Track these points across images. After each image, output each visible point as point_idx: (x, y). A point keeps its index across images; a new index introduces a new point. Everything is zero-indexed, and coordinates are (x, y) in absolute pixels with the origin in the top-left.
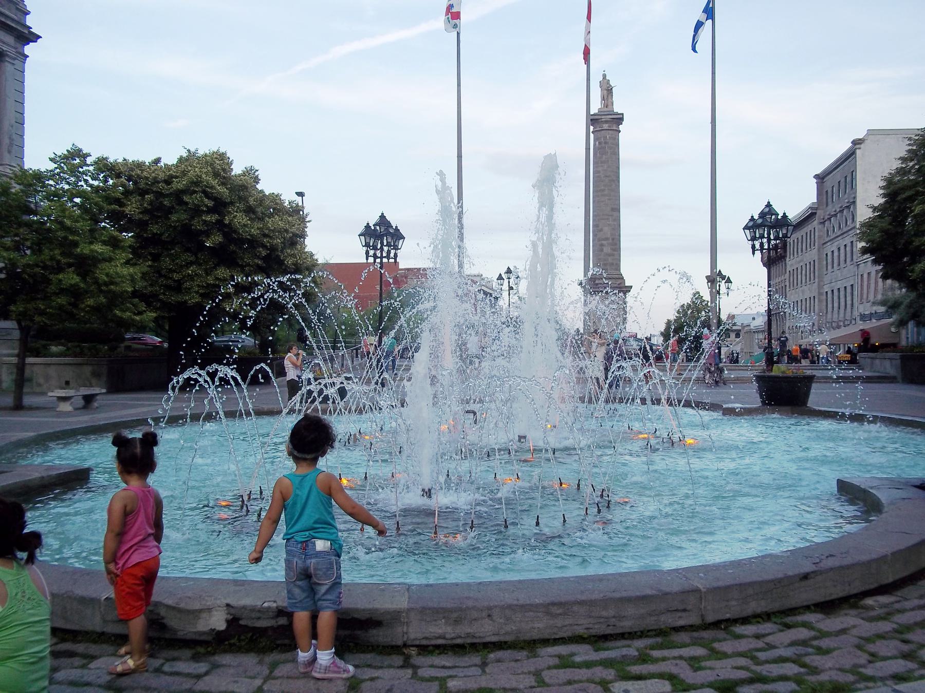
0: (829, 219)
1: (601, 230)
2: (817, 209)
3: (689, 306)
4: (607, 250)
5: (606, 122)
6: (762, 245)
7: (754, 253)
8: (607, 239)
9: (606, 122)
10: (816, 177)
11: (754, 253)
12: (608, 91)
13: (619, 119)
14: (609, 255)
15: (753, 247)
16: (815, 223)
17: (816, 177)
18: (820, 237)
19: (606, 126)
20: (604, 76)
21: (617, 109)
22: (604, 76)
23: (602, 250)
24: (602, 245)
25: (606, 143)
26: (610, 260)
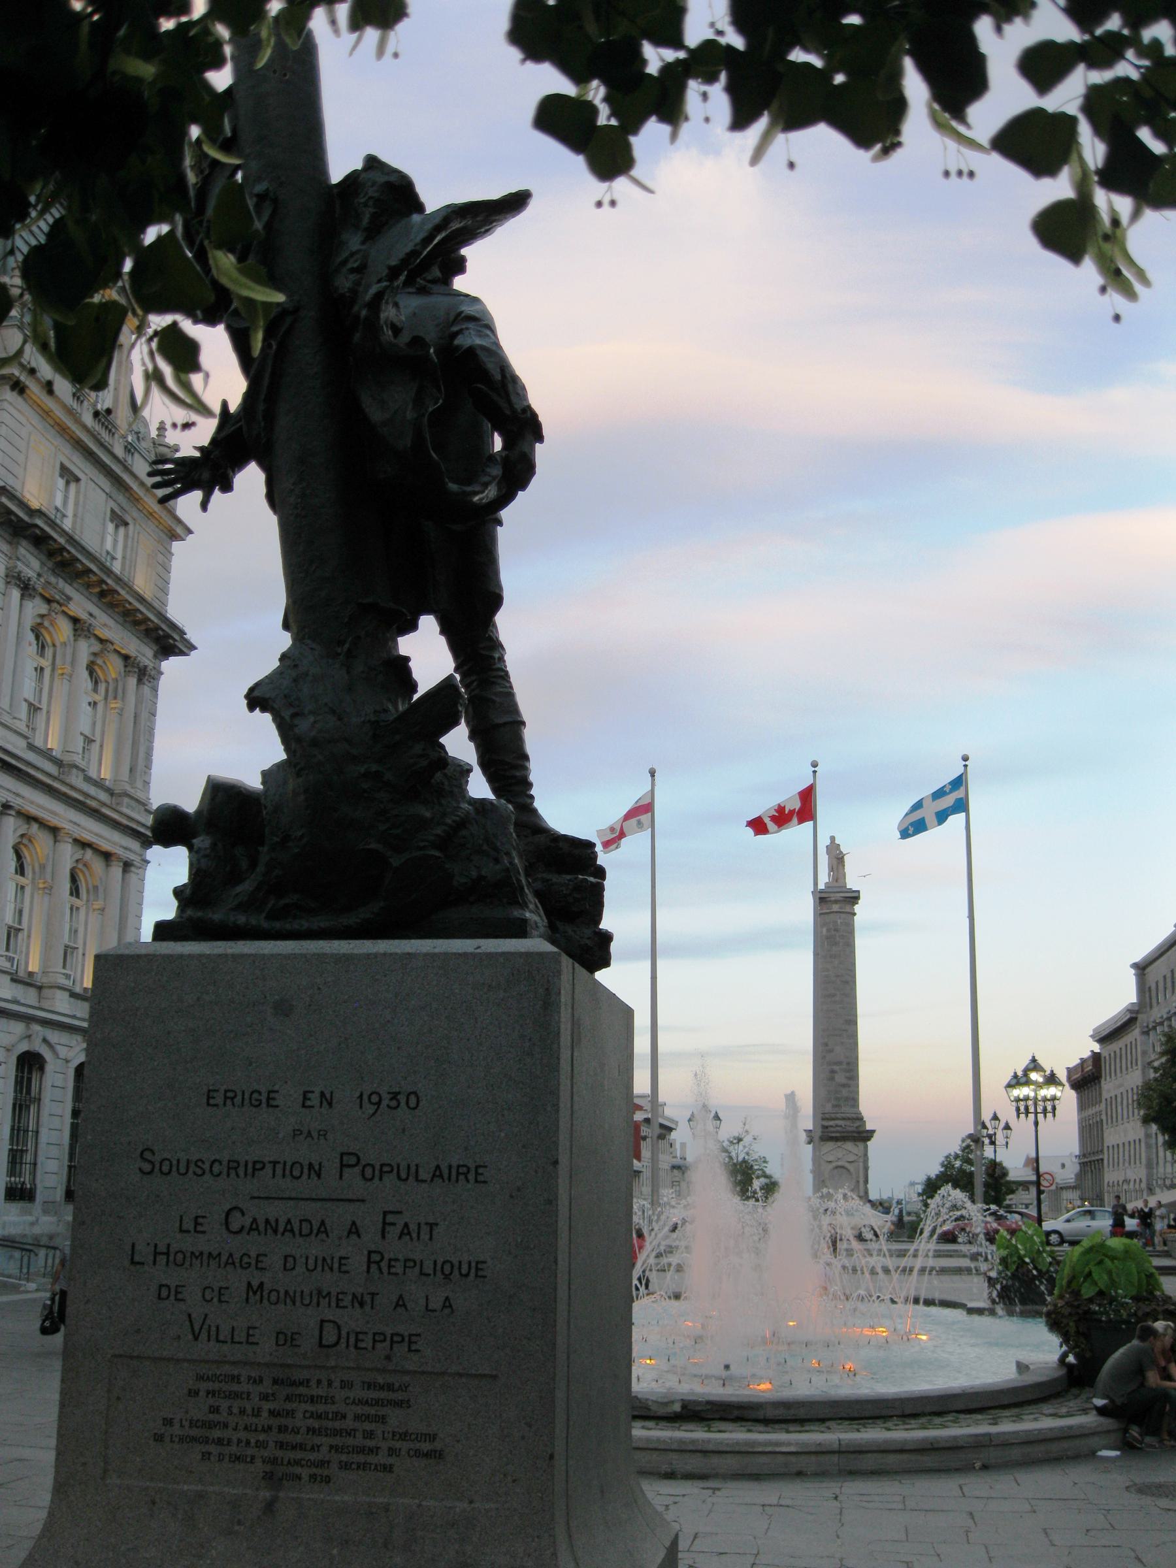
0: (1154, 1028)
1: (831, 1051)
2: (1137, 1012)
3: (957, 1157)
4: (840, 1078)
5: (836, 902)
6: (1027, 1108)
7: (1018, 1117)
8: (840, 1063)
9: (836, 902)
10: (1135, 966)
11: (1018, 1117)
12: (837, 859)
13: (854, 898)
14: (844, 1086)
15: (1018, 1109)
16: (1135, 1034)
17: (1135, 966)
18: (1144, 1053)
19: (835, 907)
20: (833, 839)
21: (852, 883)
22: (833, 839)
23: (832, 1079)
24: (833, 1072)
25: (836, 930)
26: (845, 1092)
